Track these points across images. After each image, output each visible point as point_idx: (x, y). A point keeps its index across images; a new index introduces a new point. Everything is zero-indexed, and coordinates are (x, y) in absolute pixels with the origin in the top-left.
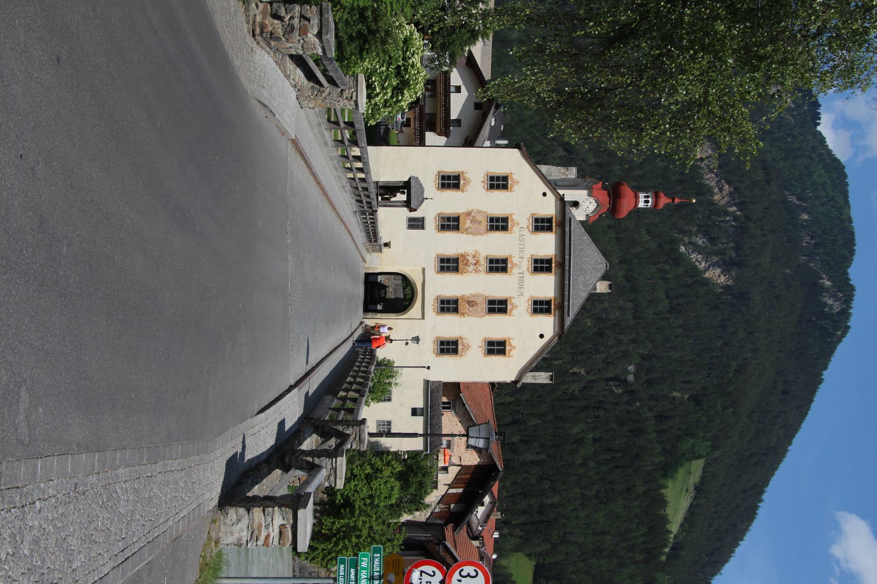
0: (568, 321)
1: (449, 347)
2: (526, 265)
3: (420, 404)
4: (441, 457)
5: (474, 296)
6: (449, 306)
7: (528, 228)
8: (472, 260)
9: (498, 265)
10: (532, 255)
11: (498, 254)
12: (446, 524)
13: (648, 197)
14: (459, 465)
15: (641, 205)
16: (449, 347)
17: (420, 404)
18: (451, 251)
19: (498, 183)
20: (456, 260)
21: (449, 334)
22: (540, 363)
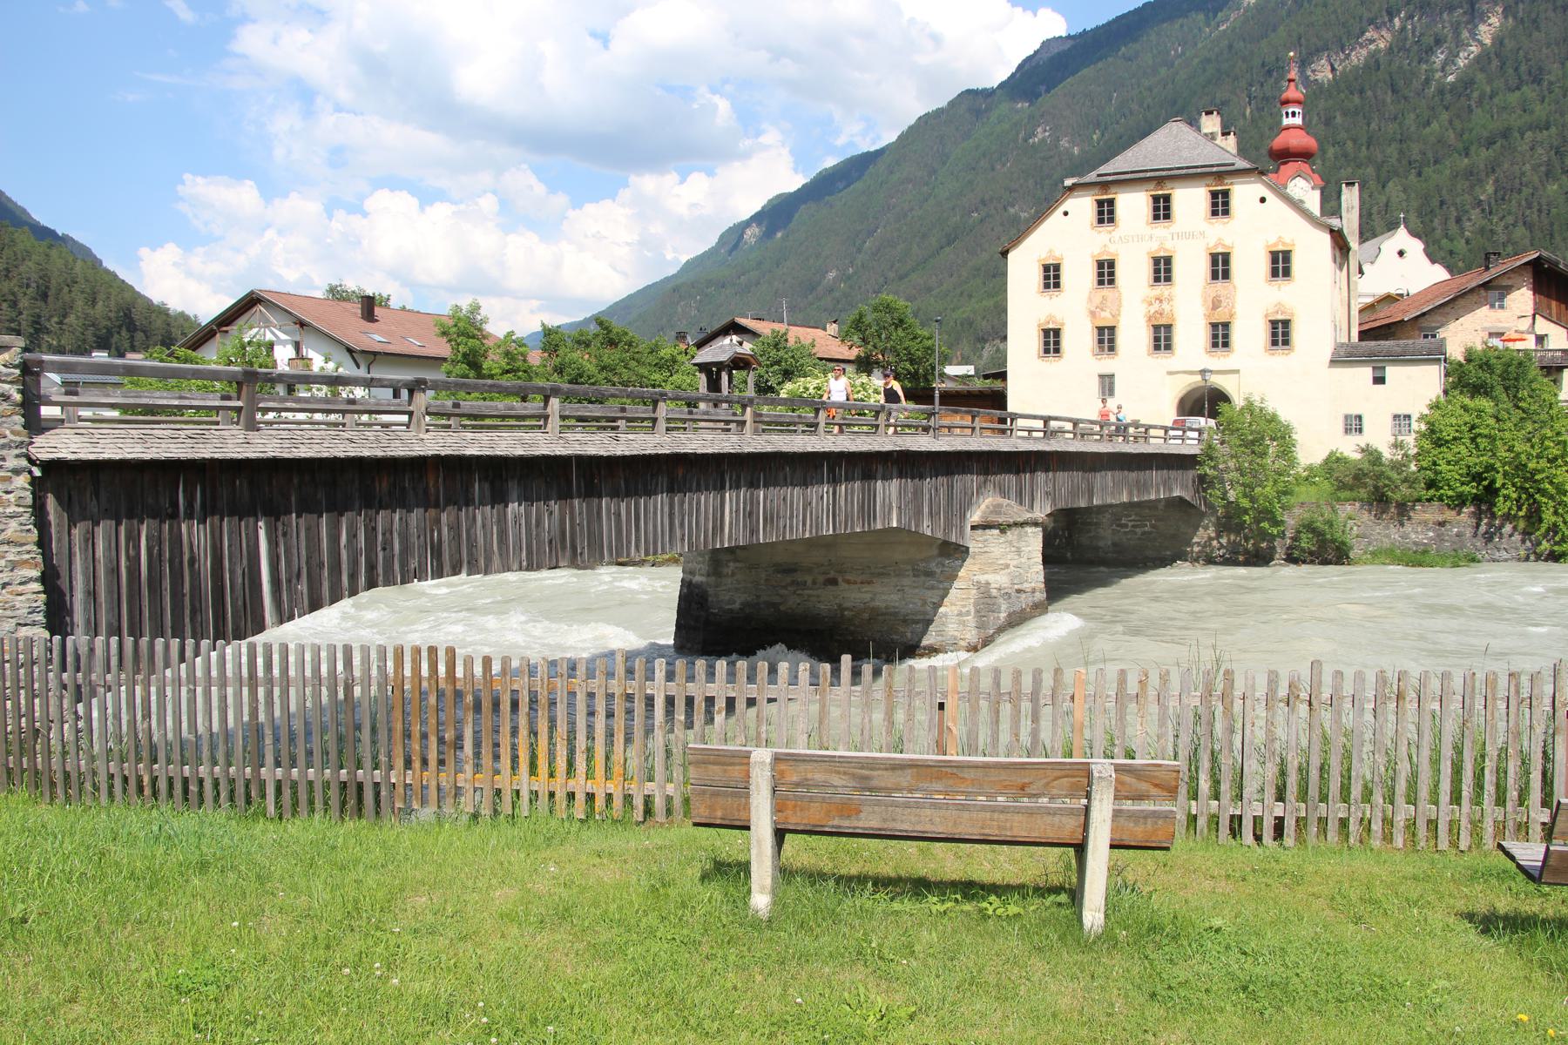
1: (1280, 333)
2: (1161, 228)
3: (1366, 373)
4: (1519, 345)
5: (1205, 301)
6: (1220, 336)
7: (1110, 232)
8: (1156, 306)
9: (1162, 269)
10: (1148, 224)
11: (1147, 270)
13: (1287, 114)
14: (1534, 319)
15: (1298, 121)
16: (1280, 333)
17: (1366, 373)
18: (1145, 337)
19: (1052, 276)
20: (1156, 328)
21: (1262, 334)
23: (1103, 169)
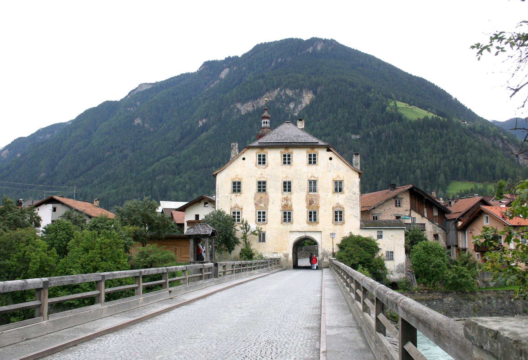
0: (321, 143)
5: (306, 200)
6: (313, 217)
8: (285, 202)
9: (287, 186)
12: (445, 217)
14: (410, 211)
15: (268, 125)
19: (237, 187)
21: (331, 216)
22: (349, 162)
23: (261, 140)
